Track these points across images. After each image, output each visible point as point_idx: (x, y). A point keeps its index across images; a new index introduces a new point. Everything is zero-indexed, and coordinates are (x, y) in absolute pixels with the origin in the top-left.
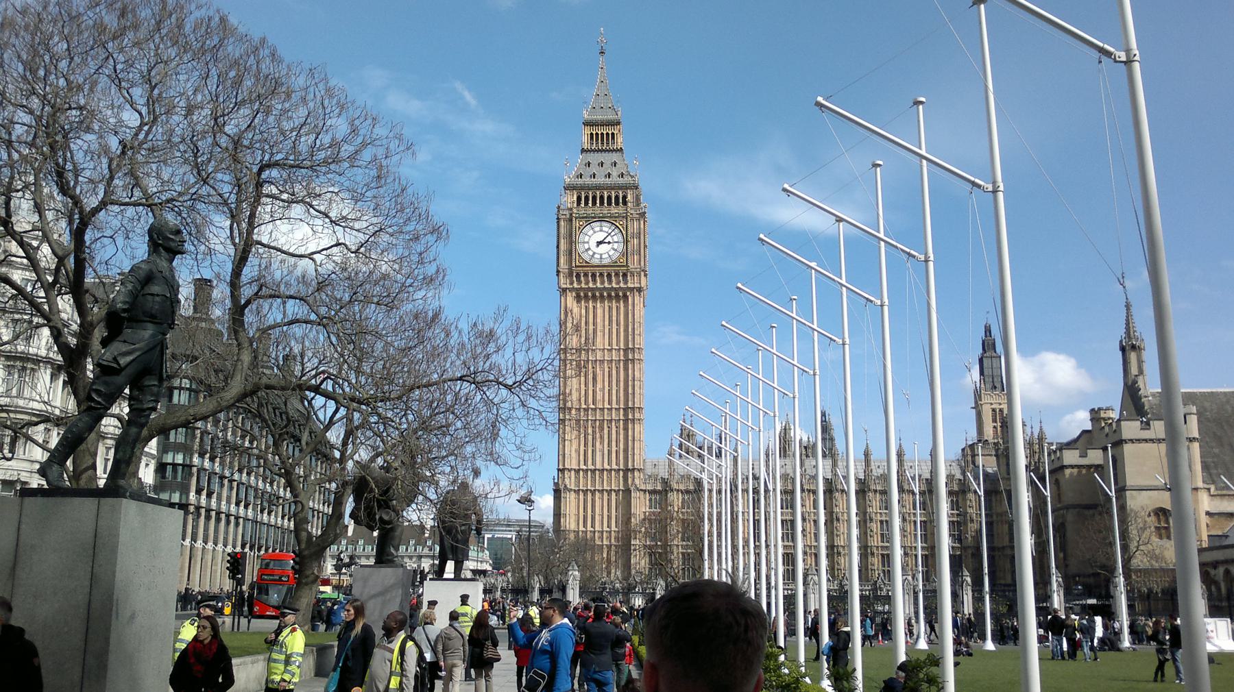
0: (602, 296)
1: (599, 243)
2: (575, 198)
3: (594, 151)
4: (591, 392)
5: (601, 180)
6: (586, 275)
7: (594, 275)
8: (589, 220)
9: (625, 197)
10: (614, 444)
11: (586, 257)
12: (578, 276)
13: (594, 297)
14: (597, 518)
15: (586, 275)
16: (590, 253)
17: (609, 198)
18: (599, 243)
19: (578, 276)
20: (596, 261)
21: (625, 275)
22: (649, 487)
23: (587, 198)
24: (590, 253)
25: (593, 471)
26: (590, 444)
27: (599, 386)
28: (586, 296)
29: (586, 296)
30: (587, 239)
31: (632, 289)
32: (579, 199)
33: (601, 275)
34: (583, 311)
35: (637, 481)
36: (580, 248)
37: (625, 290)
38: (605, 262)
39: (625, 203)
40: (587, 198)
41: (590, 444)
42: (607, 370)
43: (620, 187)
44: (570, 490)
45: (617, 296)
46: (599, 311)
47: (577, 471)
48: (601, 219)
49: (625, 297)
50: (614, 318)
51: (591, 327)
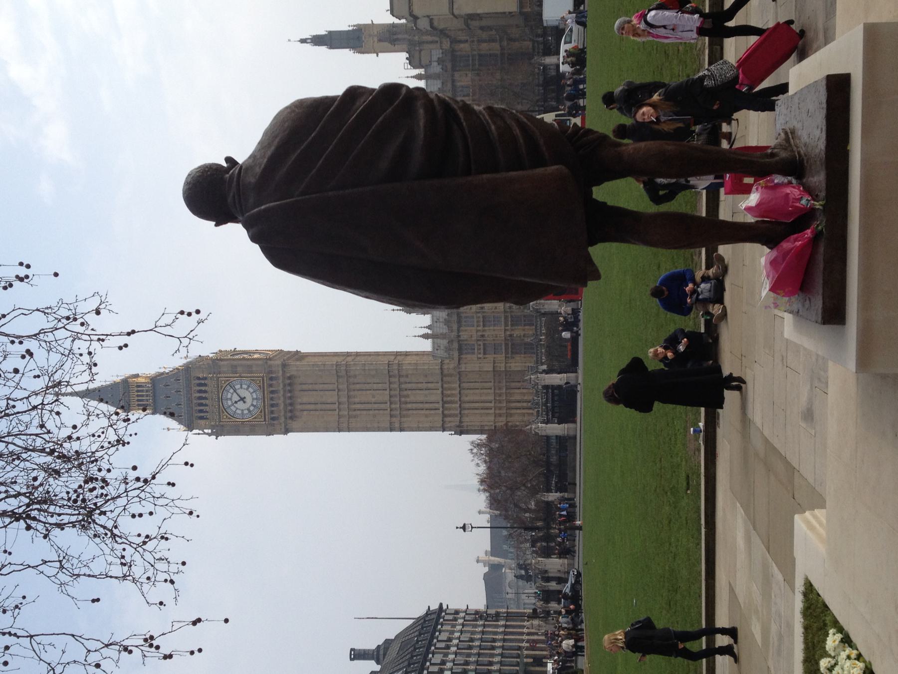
0: (290, 398)
1: (243, 399)
2: (199, 421)
4: (376, 406)
6: (272, 412)
7: (272, 405)
8: (222, 410)
9: (199, 378)
10: (420, 386)
11: (256, 412)
12: (273, 419)
13: (291, 404)
14: (484, 398)
15: (272, 412)
16: (252, 408)
19: (273, 419)
20: (260, 404)
21: (271, 379)
23: (201, 411)
24: (252, 408)
25: (444, 402)
26: (421, 406)
28: (291, 411)
29: (291, 411)
31: (284, 372)
32: (202, 418)
33: (272, 399)
34: (305, 413)
35: (452, 366)
38: (260, 396)
39: (205, 379)
40: (201, 411)
41: (421, 406)
42: (356, 392)
44: (461, 422)
45: (290, 385)
46: (305, 400)
47: (444, 416)
48: (220, 399)
49: (290, 378)
51: (319, 406)
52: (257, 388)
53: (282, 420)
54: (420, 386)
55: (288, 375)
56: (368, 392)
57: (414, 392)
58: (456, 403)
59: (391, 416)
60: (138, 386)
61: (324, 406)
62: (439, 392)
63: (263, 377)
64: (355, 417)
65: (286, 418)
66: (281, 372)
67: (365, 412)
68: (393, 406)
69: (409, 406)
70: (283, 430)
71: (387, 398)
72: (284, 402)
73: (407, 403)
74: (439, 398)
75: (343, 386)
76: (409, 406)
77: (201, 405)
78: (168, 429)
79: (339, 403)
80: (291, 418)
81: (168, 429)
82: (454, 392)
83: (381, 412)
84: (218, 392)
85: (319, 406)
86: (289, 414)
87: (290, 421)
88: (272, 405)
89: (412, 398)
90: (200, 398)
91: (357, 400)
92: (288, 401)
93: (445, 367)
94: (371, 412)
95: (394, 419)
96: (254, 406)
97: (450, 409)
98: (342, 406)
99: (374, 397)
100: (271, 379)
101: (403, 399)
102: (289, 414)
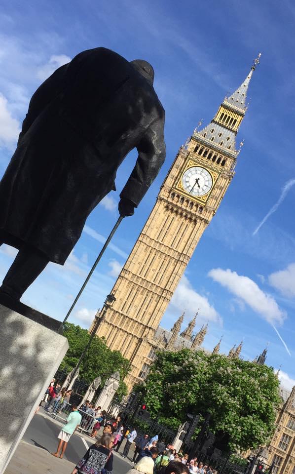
0: (181, 214)
1: (197, 180)
2: (195, 146)
3: (220, 125)
5: (216, 145)
7: (183, 199)
8: (197, 164)
11: (184, 185)
12: (173, 194)
16: (188, 184)
17: (215, 157)
18: (197, 180)
20: (187, 191)
21: (201, 208)
22: (154, 344)
23: (201, 151)
24: (188, 184)
27: (154, 267)
30: (190, 175)
31: (202, 219)
35: (149, 336)
36: (183, 178)
37: (197, 217)
38: (193, 194)
39: (223, 164)
40: (201, 151)
43: (224, 154)
44: (107, 322)
45: (190, 219)
46: (175, 223)
48: (204, 167)
49: (195, 222)
50: (182, 231)
52: (200, 195)
53: (170, 200)
55: (198, 221)
56: (159, 268)
57: (143, 300)
58: (120, 325)
59: (133, 274)
61: (164, 233)
62: (134, 318)
63: (206, 203)
64: (146, 250)
65: (169, 203)
66: (203, 217)
67: (146, 258)
68: (140, 280)
69: (134, 292)
70: (162, 197)
71: (148, 279)
72: (181, 208)
73: (138, 290)
74: (130, 316)
75: (171, 253)
76: (134, 292)
77: (206, 153)
79: (160, 244)
80: (167, 207)
82: (129, 327)
83: (140, 270)
84: (211, 169)
85: (166, 230)
86: (170, 207)
87: (166, 204)
88: (183, 199)
89: (139, 296)
90: (210, 155)
91: (157, 257)
92: (180, 211)
93: (151, 331)
94: (144, 263)
95: (131, 275)
96: (188, 187)
97: (118, 318)
98: (158, 244)
99: (153, 270)
100: (201, 208)
101: (142, 289)
102: (170, 207)
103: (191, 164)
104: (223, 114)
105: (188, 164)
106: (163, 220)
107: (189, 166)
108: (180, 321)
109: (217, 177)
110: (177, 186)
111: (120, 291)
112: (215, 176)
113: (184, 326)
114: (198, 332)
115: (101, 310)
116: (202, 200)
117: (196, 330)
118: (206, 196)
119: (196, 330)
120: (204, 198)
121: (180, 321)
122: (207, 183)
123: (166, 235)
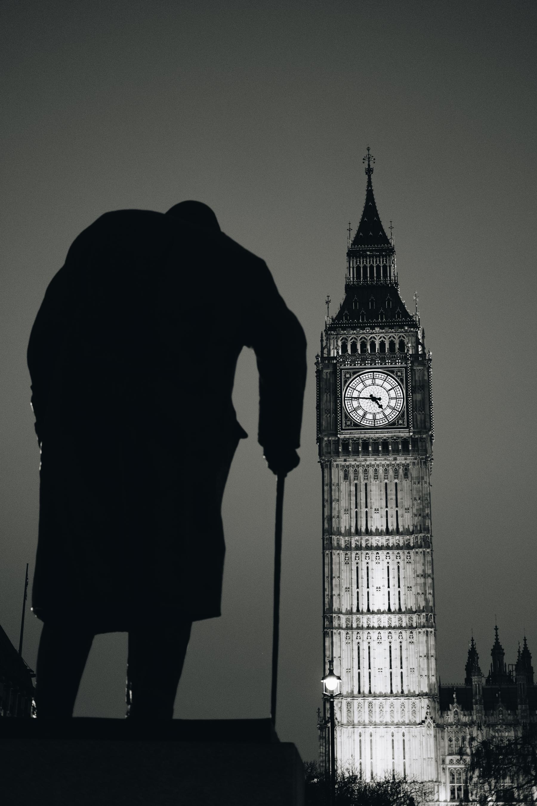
1: (373, 399)
34: (353, 489)
41: (365, 663)
54: (396, 663)
60: (385, 267)
78: (327, 302)
81: (327, 302)
103: (348, 376)
104: (358, 268)
105: (343, 377)
106: (350, 495)
107: (346, 382)
108: (473, 654)
109: (404, 375)
110: (344, 425)
111: (340, 657)
112: (399, 374)
113: (485, 663)
114: (514, 661)
115: (322, 710)
116: (400, 426)
117: (511, 659)
118: (403, 415)
119: (511, 659)
120: (400, 422)
121: (473, 654)
122: (392, 394)
123: (369, 519)
